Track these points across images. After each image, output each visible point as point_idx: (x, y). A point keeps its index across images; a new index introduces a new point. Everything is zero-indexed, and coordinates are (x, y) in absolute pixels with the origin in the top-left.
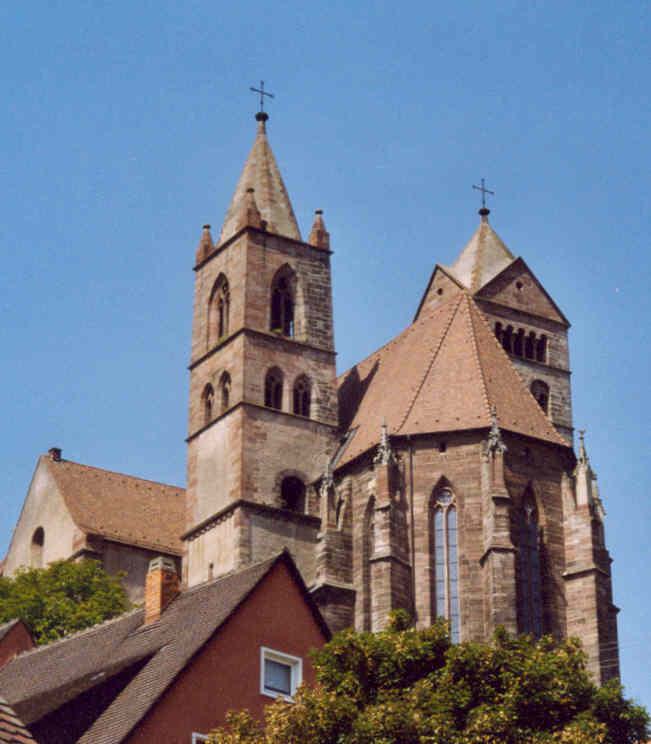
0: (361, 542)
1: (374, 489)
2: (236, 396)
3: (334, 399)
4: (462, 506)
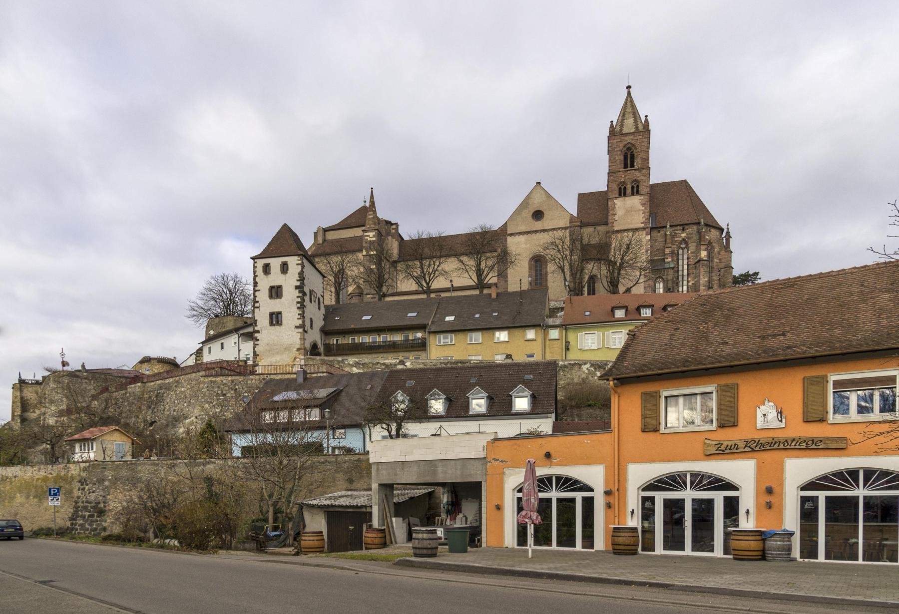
0: (676, 252)
1: (685, 236)
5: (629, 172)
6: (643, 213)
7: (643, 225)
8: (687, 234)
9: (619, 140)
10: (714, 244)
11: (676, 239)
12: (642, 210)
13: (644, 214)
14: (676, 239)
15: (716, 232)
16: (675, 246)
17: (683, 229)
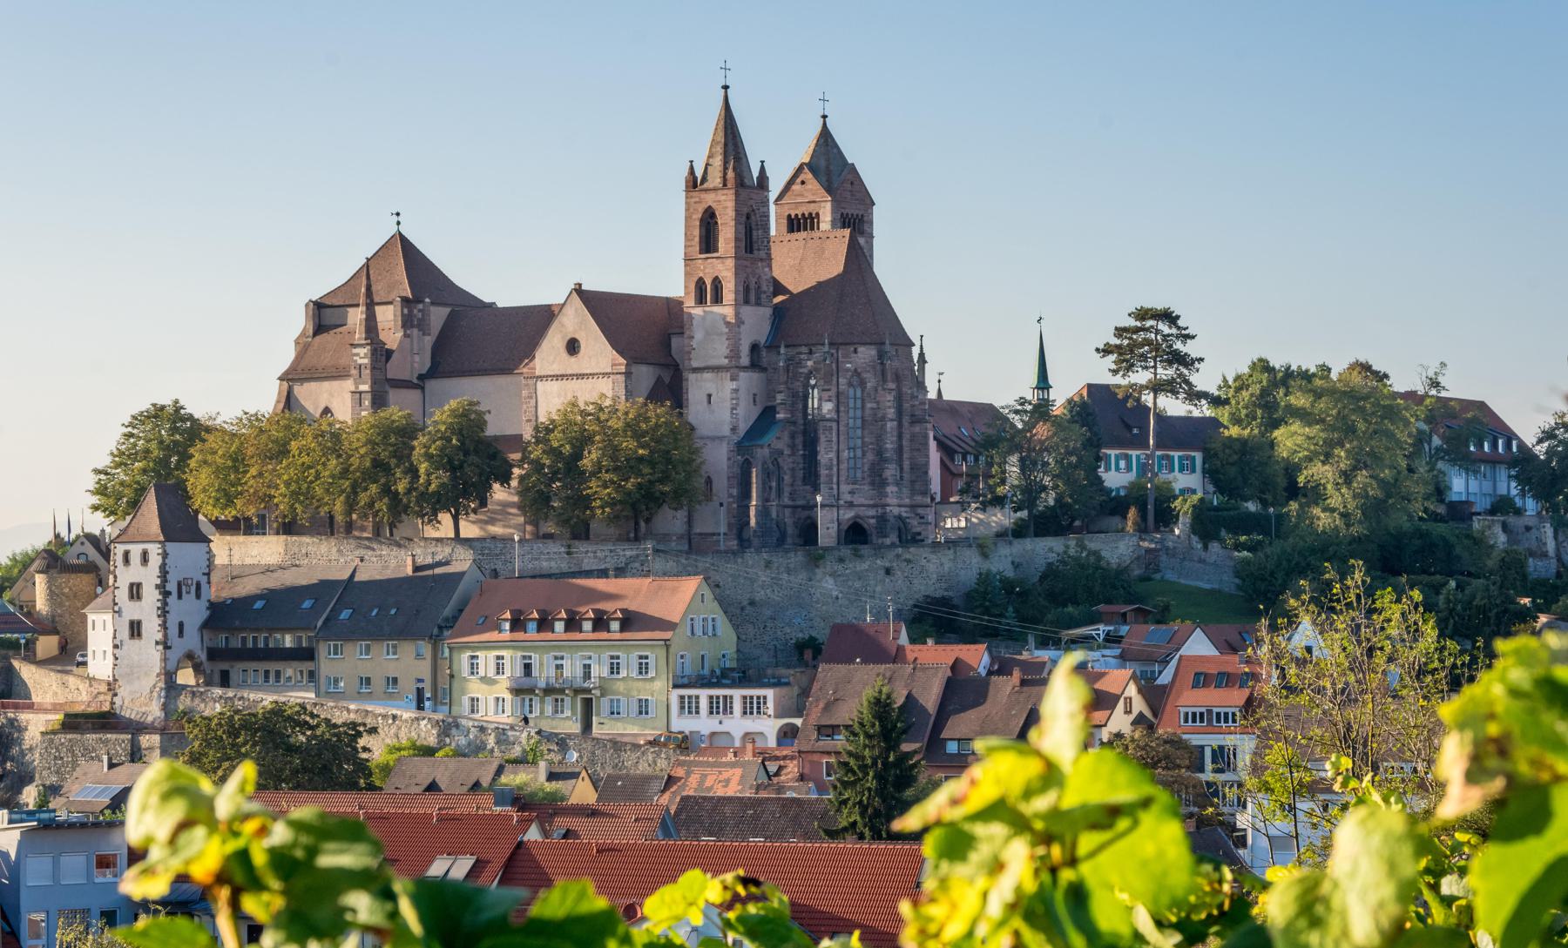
0: (801, 394)
2: (729, 294)
3: (771, 289)
5: (709, 261)
7: (726, 361)
9: (697, 200)
10: (865, 375)
11: (801, 370)
14: (801, 370)
17: (811, 352)
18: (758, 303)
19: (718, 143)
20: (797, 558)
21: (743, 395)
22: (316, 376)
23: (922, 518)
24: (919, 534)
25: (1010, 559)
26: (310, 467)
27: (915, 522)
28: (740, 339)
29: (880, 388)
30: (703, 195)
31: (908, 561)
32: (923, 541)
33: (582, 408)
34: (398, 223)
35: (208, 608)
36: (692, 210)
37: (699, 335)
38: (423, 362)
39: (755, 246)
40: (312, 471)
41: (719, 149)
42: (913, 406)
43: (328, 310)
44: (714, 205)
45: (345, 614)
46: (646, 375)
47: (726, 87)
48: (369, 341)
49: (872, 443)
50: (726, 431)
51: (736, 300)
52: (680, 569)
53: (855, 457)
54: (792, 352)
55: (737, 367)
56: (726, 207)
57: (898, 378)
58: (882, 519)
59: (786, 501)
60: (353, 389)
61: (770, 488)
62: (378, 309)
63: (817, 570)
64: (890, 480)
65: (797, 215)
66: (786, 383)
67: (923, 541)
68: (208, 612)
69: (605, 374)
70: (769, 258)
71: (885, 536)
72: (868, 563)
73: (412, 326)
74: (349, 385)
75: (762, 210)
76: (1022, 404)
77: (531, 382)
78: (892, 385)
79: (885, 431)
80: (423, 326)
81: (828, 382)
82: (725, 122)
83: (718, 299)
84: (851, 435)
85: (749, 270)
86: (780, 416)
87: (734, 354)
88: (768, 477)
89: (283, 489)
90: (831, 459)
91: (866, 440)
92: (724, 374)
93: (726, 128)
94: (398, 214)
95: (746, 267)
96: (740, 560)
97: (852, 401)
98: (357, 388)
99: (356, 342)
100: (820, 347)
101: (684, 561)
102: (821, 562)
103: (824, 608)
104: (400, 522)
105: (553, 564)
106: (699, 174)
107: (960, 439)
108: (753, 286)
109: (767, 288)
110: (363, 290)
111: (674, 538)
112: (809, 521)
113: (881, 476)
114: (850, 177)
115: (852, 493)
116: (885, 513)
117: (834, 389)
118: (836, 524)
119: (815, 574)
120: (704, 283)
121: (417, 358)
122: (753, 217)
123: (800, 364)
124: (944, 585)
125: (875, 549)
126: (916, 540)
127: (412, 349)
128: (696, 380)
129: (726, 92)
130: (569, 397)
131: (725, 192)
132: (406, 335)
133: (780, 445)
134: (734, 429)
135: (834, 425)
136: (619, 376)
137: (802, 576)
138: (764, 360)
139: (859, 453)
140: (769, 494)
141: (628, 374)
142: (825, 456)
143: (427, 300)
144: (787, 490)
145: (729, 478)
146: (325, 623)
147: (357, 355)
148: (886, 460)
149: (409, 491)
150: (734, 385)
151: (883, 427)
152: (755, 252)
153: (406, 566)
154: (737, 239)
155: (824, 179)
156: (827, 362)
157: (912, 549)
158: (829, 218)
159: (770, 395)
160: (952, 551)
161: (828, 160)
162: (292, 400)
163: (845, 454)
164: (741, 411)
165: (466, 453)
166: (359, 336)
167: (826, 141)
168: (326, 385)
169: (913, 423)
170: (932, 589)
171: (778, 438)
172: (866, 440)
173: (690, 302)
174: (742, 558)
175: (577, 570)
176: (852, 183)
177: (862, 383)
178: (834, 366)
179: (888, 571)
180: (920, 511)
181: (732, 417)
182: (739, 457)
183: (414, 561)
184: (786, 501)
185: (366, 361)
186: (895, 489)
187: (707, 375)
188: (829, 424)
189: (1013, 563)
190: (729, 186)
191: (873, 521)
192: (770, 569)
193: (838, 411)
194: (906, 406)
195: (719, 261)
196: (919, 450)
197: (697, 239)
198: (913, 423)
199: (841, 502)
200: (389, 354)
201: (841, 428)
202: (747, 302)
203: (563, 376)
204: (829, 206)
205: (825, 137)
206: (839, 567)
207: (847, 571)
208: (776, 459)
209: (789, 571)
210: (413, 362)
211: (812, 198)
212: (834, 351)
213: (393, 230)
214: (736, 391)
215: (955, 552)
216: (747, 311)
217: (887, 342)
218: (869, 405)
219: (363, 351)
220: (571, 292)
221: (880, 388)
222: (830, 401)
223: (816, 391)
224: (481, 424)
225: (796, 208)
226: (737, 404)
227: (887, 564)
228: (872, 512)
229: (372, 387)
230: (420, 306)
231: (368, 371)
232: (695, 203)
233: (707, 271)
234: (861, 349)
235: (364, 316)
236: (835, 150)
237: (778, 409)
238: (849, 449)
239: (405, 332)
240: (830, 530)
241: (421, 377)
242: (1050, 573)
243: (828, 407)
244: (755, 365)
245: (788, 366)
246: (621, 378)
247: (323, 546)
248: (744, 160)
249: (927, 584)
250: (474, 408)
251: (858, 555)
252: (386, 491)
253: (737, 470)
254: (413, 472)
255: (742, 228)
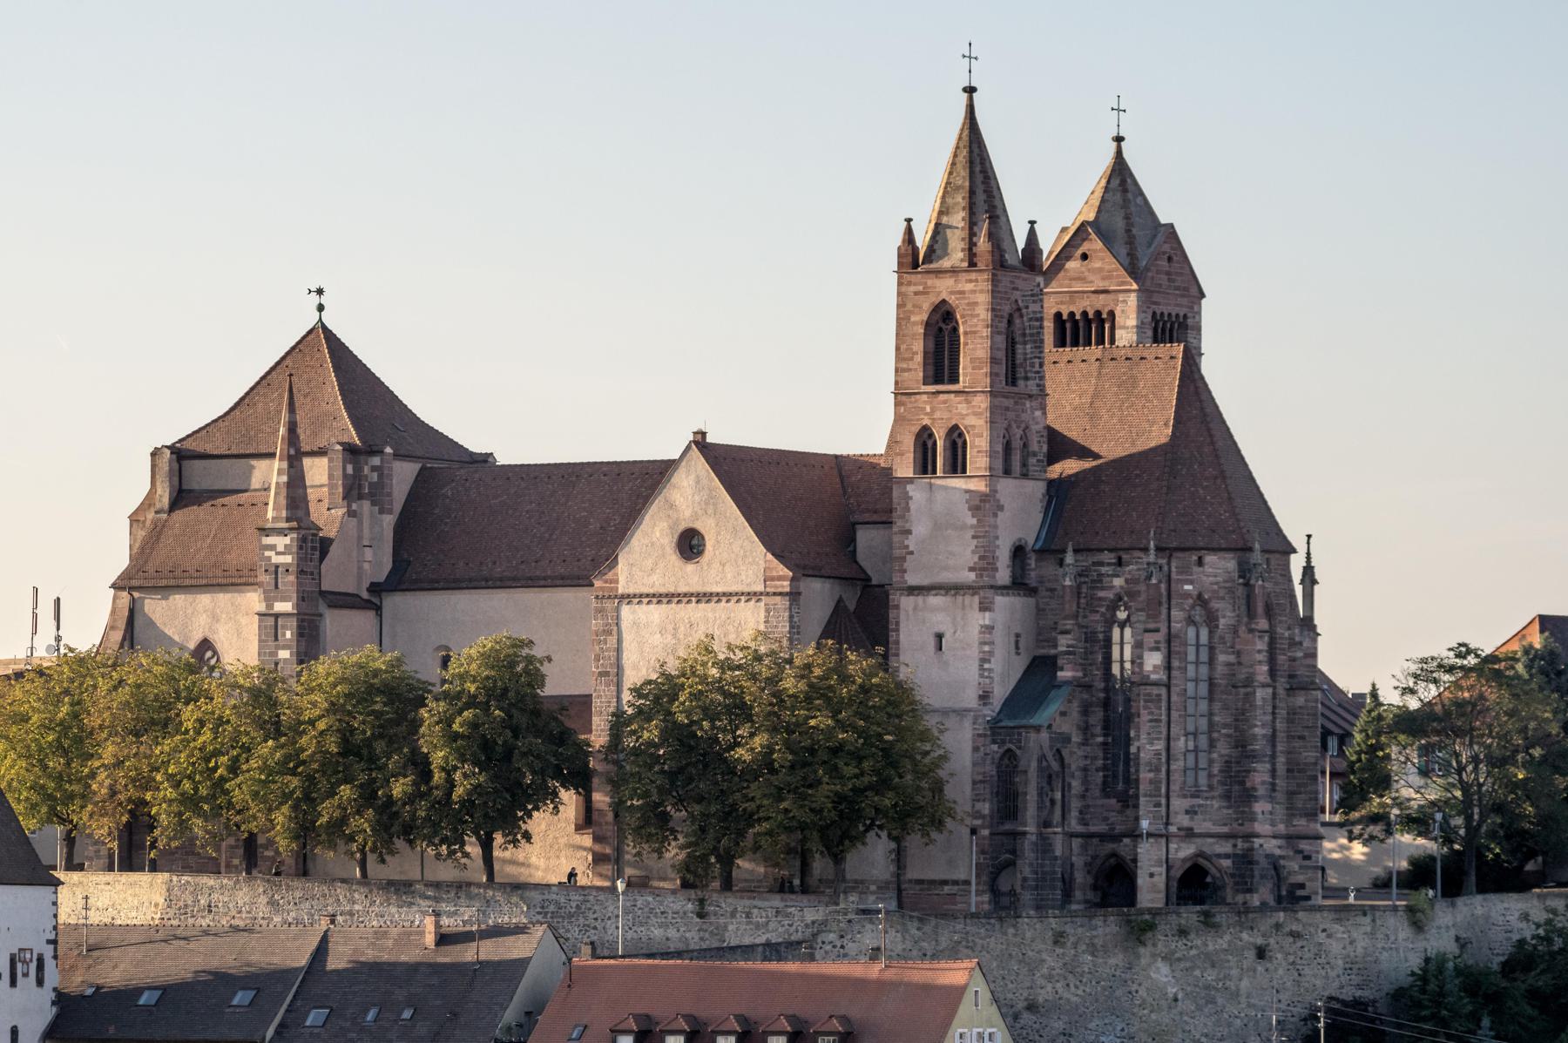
0: (1101, 636)
1: (1121, 587)
3: (1045, 448)
4: (1217, 626)
5: (942, 397)
6: (974, 537)
7: (972, 576)
8: (1127, 581)
9: (921, 288)
10: (1215, 605)
11: (1101, 594)
12: (972, 526)
13: (975, 542)
14: (1101, 594)
15: (1222, 564)
16: (1097, 617)
17: (1120, 563)
18: (1025, 476)
19: (958, 188)
20: (1107, 927)
21: (999, 636)
22: (188, 582)
23: (1308, 858)
24: (1302, 886)
25: (1453, 933)
26: (217, 753)
27: (1293, 865)
28: (997, 538)
29: (1243, 629)
30: (931, 281)
31: (1296, 935)
32: (1308, 898)
33: (721, 657)
34: (321, 308)
35: (53, 1003)
36: (909, 307)
37: (920, 528)
38: (378, 563)
39: (1020, 373)
40: (224, 759)
41: (960, 199)
42: (1294, 660)
43: (197, 463)
44: (952, 300)
45: (315, 1017)
46: (821, 595)
47: (970, 90)
48: (294, 524)
49: (1226, 726)
50: (970, 699)
51: (991, 469)
52: (909, 945)
53: (1196, 750)
54: (1089, 560)
55: (992, 587)
56: (976, 304)
57: (1269, 612)
58: (1245, 860)
59: (1074, 825)
60: (262, 608)
61: (1053, 802)
62: (307, 462)
63: (1142, 950)
64: (1261, 791)
65: (1072, 314)
66: (1076, 617)
67: (1308, 898)
68: (54, 1009)
69: (750, 595)
70: (1042, 393)
71: (1250, 891)
72: (1227, 937)
73: (361, 497)
74: (253, 600)
75: (1033, 307)
76: (1458, 656)
77: (608, 605)
78: (1263, 624)
79: (1253, 706)
80: (378, 495)
81: (1154, 617)
82: (971, 152)
83: (957, 465)
84: (1191, 710)
85: (1011, 415)
86: (1065, 674)
87: (986, 564)
88: (1049, 783)
89: (170, 793)
90: (1158, 754)
91: (1217, 719)
92: (968, 599)
93: (971, 162)
94: (320, 292)
95: (1007, 409)
96: (1011, 931)
97: (1191, 651)
98: (270, 606)
99: (269, 525)
100: (1137, 554)
101: (914, 931)
102: (1149, 934)
103: (1154, 1016)
104: (392, 853)
105: (672, 933)
106: (922, 240)
107: (1345, 709)
108: (1017, 444)
109: (1039, 447)
110: (282, 431)
111: (873, 888)
112: (1112, 861)
113: (1242, 783)
114: (1166, 247)
115: (1191, 812)
116: (1252, 849)
117: (1164, 630)
118: (1163, 869)
119: (1138, 957)
120: (931, 435)
121: (368, 554)
122: (1017, 321)
123: (1098, 582)
124: (1356, 979)
125: (1239, 913)
126: (1292, 898)
127: (360, 538)
128: (915, 609)
129: (971, 99)
130: (699, 635)
131: (973, 276)
132: (351, 513)
133: (1067, 726)
134: (985, 697)
135: (1163, 691)
136: (778, 598)
137: (1117, 959)
138: (1033, 574)
139: (1203, 741)
140: (1051, 812)
141: (794, 595)
142: (1146, 745)
143: (388, 450)
144: (1075, 804)
145: (974, 783)
146: (278, 1032)
147: (272, 547)
148: (1253, 756)
149: (411, 799)
150: (986, 618)
151: (1249, 697)
152: (1021, 383)
153: (422, 933)
154: (994, 360)
155: (1123, 251)
156: (1154, 581)
157: (1301, 915)
158: (1132, 321)
159: (1044, 633)
160: (1368, 919)
161: (1127, 217)
162: (138, 623)
163: (1180, 744)
164: (996, 664)
165: (516, 732)
166: (272, 512)
167: (1123, 182)
168: (205, 600)
169: (1291, 690)
170: (1336, 984)
171: (1063, 714)
172: (1217, 719)
173: (905, 468)
174: (1014, 926)
175: (716, 944)
176: (1170, 259)
177: (1211, 620)
178: (1163, 586)
179: (1261, 953)
180: (1304, 846)
181: (981, 676)
182: (995, 747)
183: (438, 925)
184: (1074, 825)
185: (288, 559)
186: (1268, 807)
187: (935, 600)
188: (1155, 691)
189: (1457, 939)
190: (981, 266)
191: (1226, 863)
192: (1063, 945)
193: (1168, 667)
194: (1281, 658)
195: (961, 398)
196: (1302, 738)
197: (919, 358)
198: (1291, 690)
199: (1173, 829)
200: (324, 545)
201: (1174, 698)
202: (1007, 472)
203: (673, 595)
204: (1132, 299)
205: (1120, 176)
206: (1178, 945)
207: (1193, 952)
208: (1058, 751)
209: (1093, 950)
210: (360, 562)
211: (1100, 285)
212: (1163, 561)
213: (311, 320)
214: (989, 629)
215: (1374, 921)
216: (1008, 488)
217: (1257, 546)
218: (1222, 658)
219: (281, 542)
220: (688, 448)
221: (1243, 629)
222: (1157, 649)
223: (1128, 631)
224: (537, 679)
225: (1072, 302)
226: (991, 653)
227: (1260, 941)
228: (1225, 847)
229: (298, 606)
230: (376, 461)
231: (292, 578)
232: (916, 293)
233: (937, 415)
234: (1210, 559)
235: (285, 478)
236: (1139, 200)
237: (1060, 662)
238: (1186, 735)
239: (349, 506)
240: (1156, 879)
241: (375, 588)
242: (1521, 960)
243: (1153, 660)
244: (1019, 585)
245: (1079, 586)
246: (782, 603)
247: (241, 893)
248: (1003, 219)
249: (1327, 977)
250: (525, 652)
251: (1208, 922)
252: (368, 796)
253: (991, 769)
254: (421, 766)
255: (1001, 340)
